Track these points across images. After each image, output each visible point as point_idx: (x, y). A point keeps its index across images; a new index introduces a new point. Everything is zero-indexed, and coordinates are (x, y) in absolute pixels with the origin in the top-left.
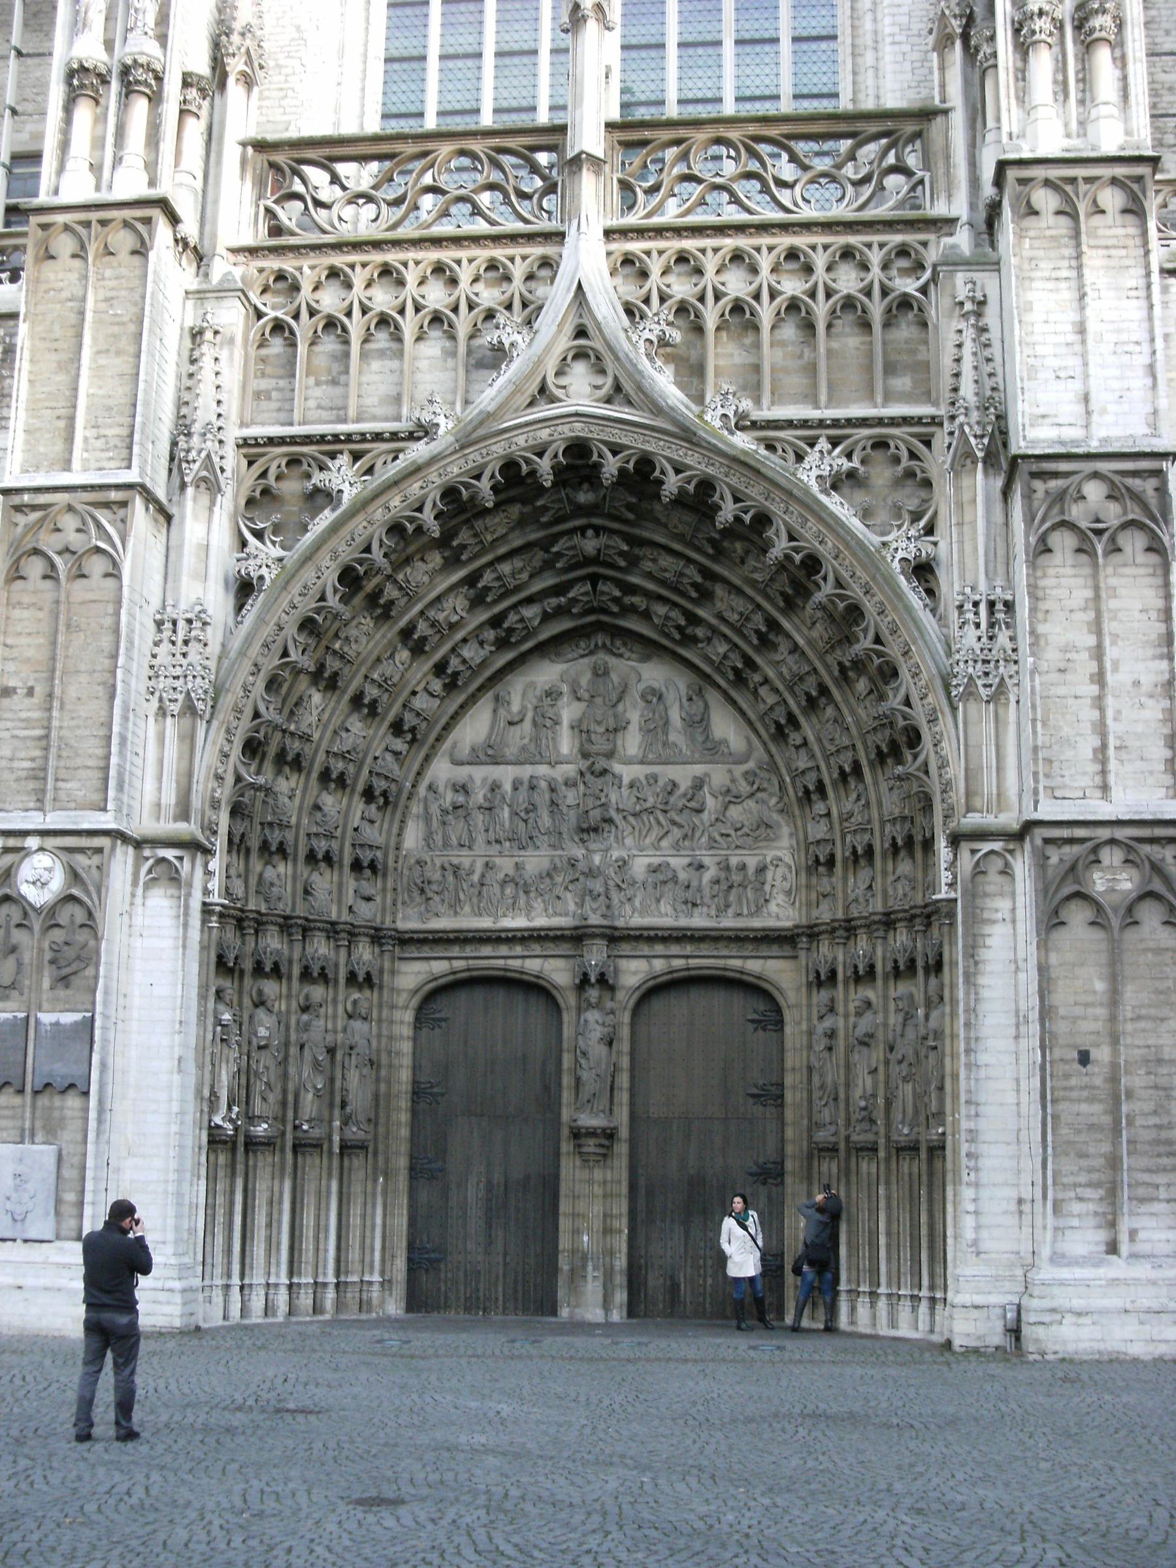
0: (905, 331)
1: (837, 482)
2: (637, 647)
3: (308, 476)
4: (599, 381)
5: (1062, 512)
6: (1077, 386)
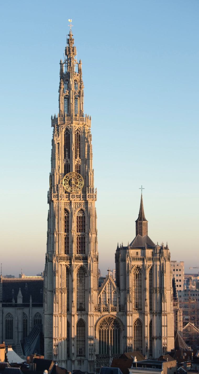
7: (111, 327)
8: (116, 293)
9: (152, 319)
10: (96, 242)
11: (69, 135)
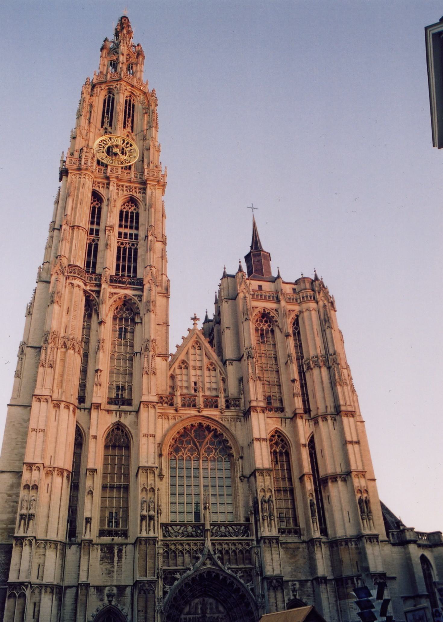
0: (247, 554)
4: (210, 562)
6: (272, 567)
8: (215, 370)
9: (313, 432)
10: (162, 257)
11: (113, 99)
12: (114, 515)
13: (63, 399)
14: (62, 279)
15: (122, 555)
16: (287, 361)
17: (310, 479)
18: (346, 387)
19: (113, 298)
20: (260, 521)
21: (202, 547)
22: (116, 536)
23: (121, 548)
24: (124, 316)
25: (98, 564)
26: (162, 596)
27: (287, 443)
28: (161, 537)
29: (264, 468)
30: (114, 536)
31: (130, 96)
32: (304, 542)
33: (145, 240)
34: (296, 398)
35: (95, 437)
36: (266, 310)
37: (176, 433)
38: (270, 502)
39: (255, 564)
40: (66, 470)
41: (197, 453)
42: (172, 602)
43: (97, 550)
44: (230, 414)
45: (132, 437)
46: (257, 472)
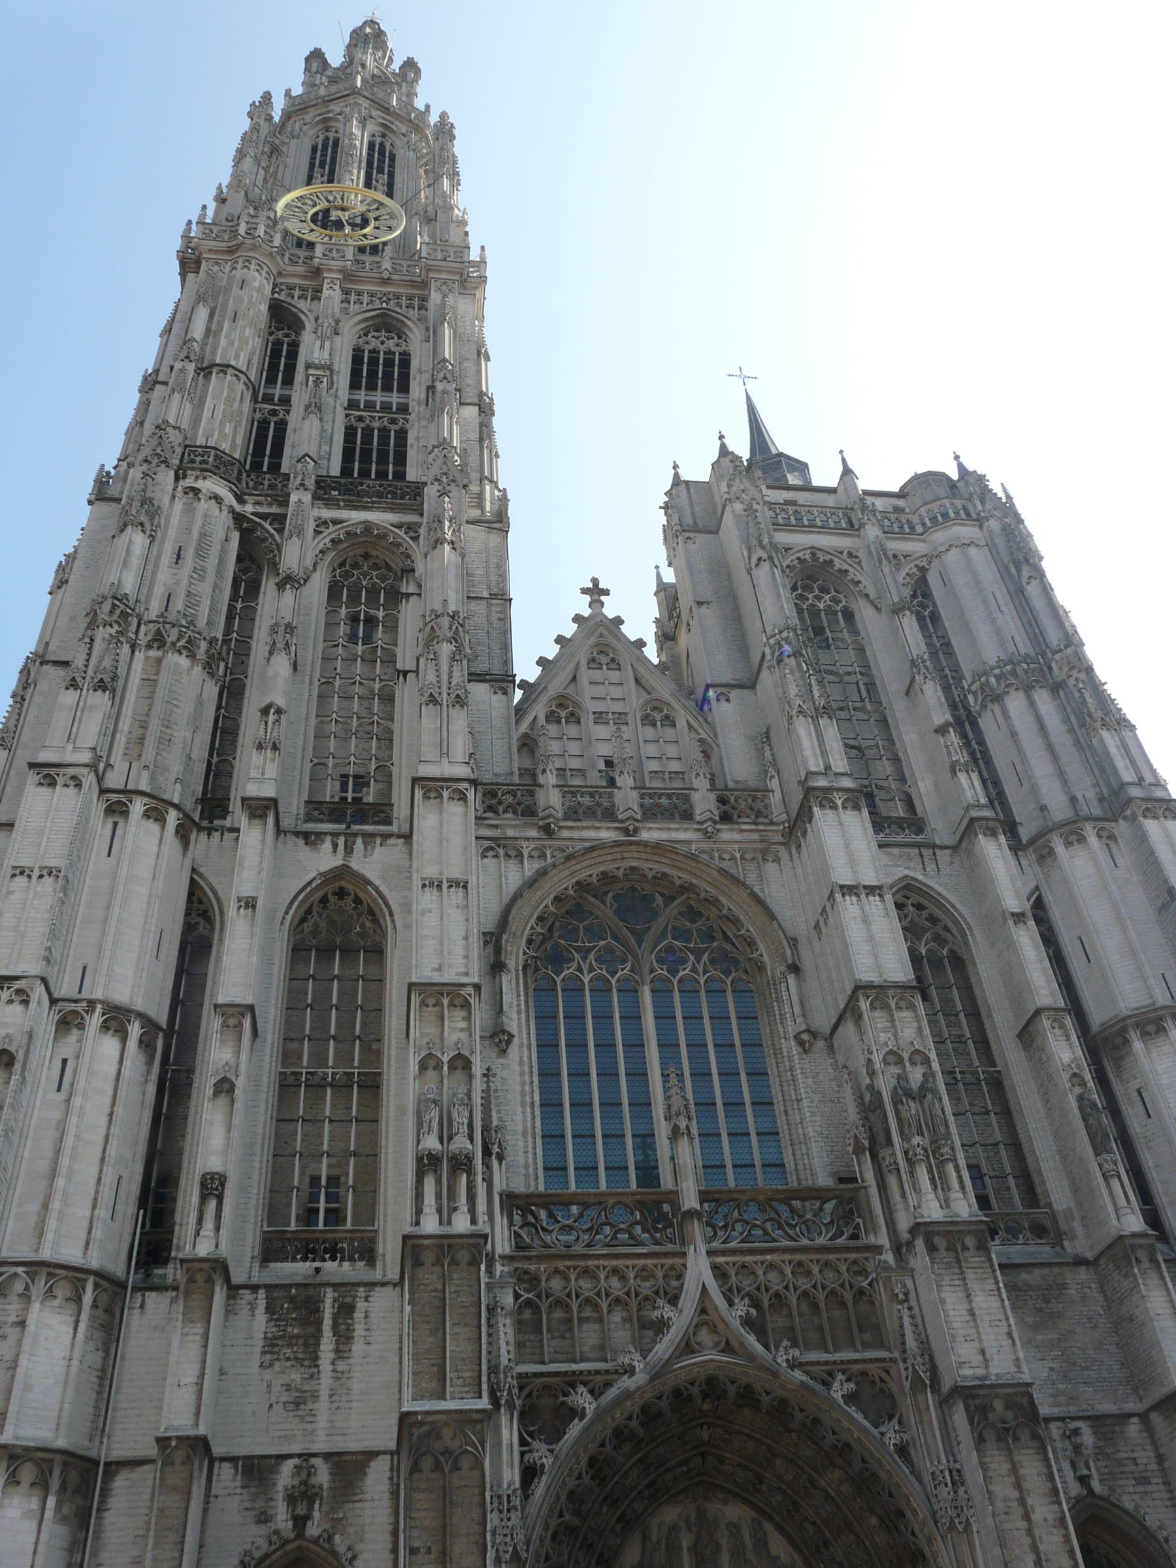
1: (850, 1398)
2: (720, 1496)
3: (556, 1397)
4: (716, 1338)
5: (986, 1418)
6: (977, 1345)
7: (660, 960)
8: (673, 725)
9: (1037, 888)
10: (481, 440)
12: (323, 1182)
13: (143, 787)
14: (166, 477)
15: (350, 1329)
16: (913, 680)
17: (1062, 1026)
18: (1131, 734)
19: (328, 531)
20: (898, 1170)
21: (674, 1283)
22: (333, 1259)
23: (348, 1300)
24: (364, 583)
25: (255, 1369)
26: (517, 1485)
27: (950, 925)
28: (502, 1243)
29: (885, 981)
30: (324, 1260)
31: (383, 136)
32: (1079, 1262)
33: (427, 405)
34: (962, 777)
35: (250, 904)
36: (819, 554)
37: (549, 901)
38: (929, 1096)
39: (904, 1343)
40: (141, 1015)
41: (628, 965)
42: (561, 1515)
43: (252, 1310)
44: (737, 836)
45: (391, 915)
46: (861, 999)
